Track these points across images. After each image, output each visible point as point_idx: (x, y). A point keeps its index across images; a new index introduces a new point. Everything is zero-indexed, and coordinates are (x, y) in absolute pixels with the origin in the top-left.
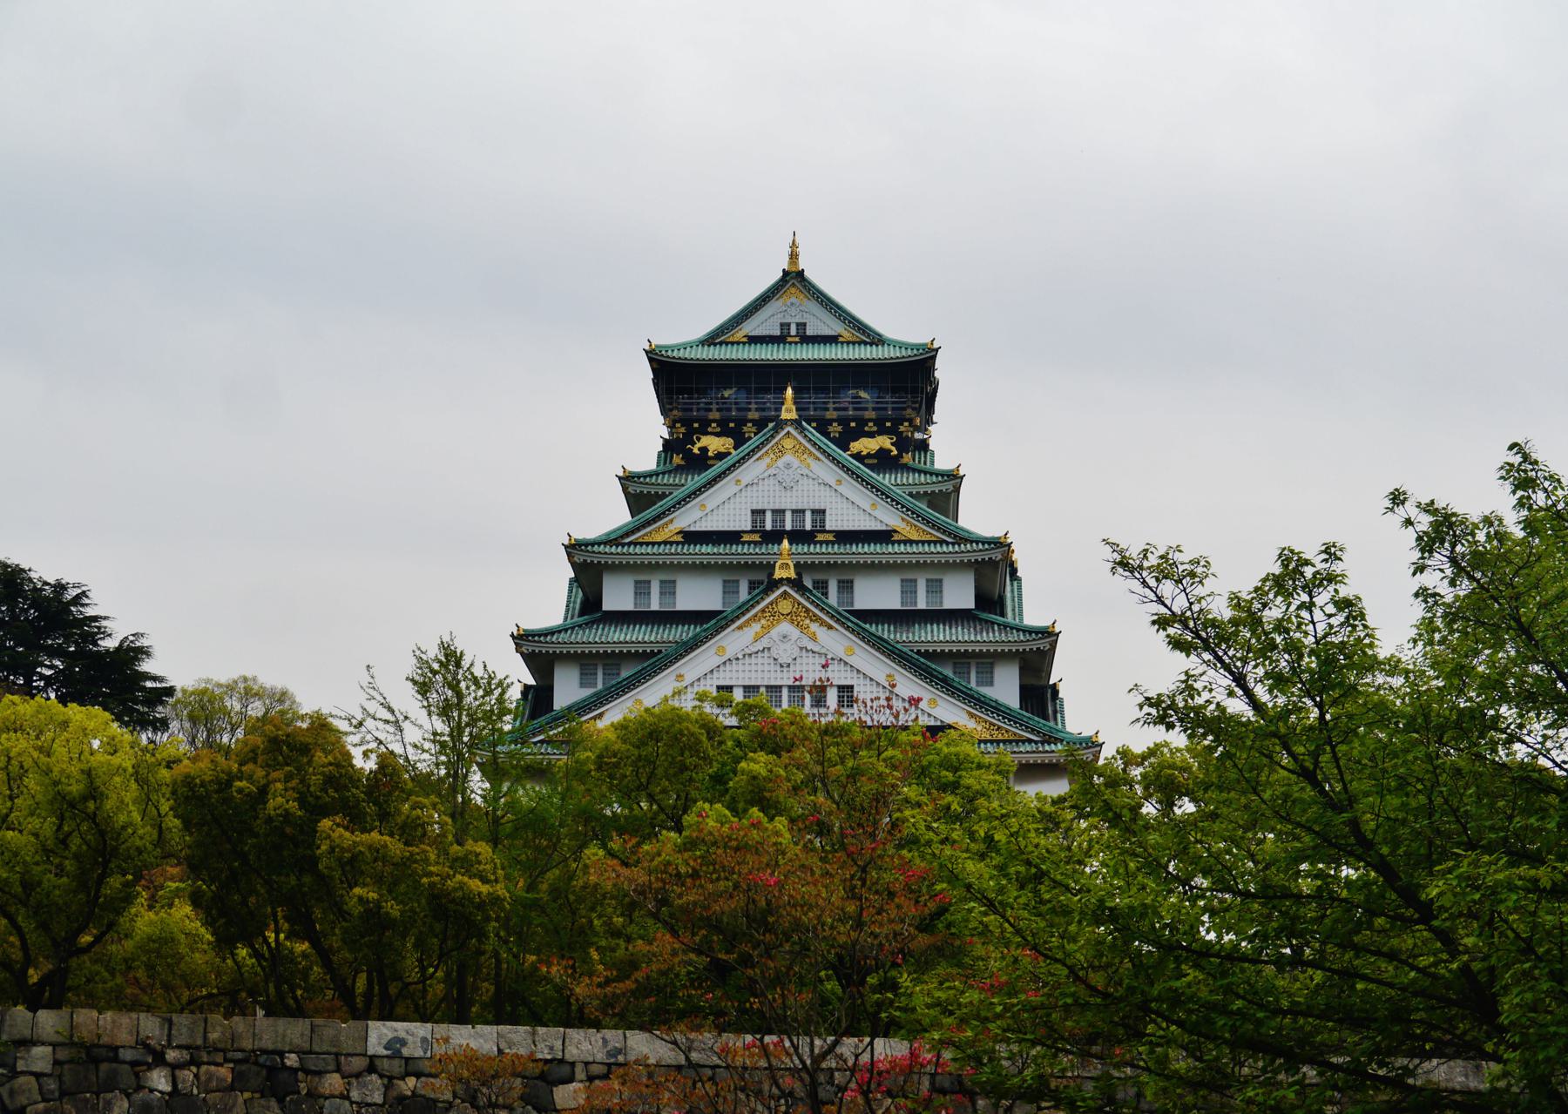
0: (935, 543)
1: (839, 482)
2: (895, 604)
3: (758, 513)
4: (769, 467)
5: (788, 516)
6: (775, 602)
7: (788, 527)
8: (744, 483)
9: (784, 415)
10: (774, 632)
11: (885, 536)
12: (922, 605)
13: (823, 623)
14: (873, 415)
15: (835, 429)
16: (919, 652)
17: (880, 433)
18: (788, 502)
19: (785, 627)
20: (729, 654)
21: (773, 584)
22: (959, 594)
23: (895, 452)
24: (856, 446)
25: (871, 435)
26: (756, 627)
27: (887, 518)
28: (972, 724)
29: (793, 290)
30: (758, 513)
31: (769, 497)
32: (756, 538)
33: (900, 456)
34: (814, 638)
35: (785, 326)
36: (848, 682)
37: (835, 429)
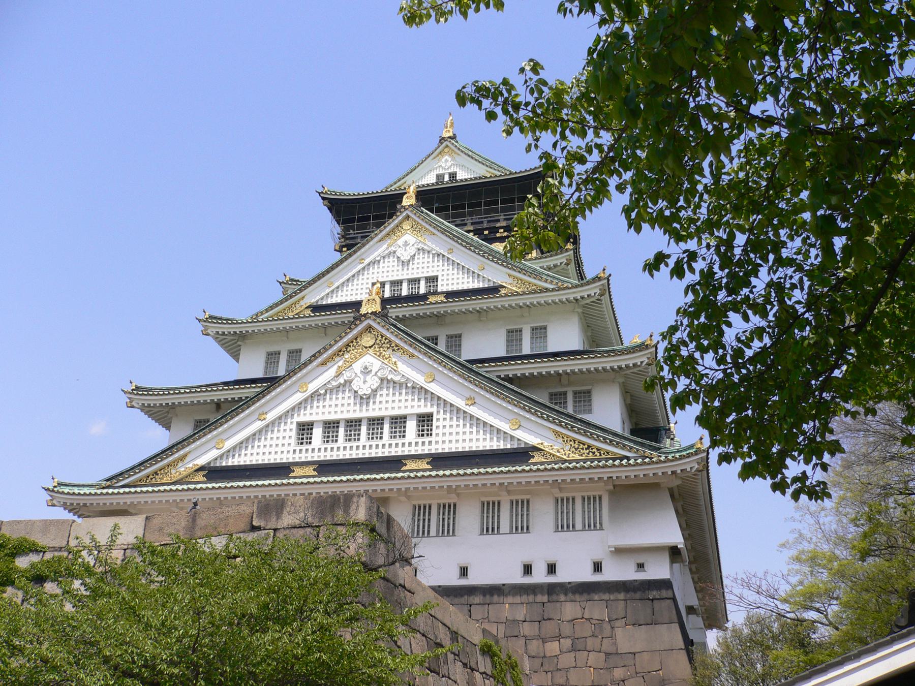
0: (541, 291)
2: (502, 353)
5: (405, 285)
7: (405, 293)
10: (357, 366)
11: (493, 290)
12: (526, 350)
13: (405, 352)
14: (504, 224)
19: (370, 360)
20: (312, 387)
21: (359, 318)
22: (566, 336)
27: (497, 275)
29: (446, 150)
31: (389, 271)
35: (440, 177)
36: (428, 410)
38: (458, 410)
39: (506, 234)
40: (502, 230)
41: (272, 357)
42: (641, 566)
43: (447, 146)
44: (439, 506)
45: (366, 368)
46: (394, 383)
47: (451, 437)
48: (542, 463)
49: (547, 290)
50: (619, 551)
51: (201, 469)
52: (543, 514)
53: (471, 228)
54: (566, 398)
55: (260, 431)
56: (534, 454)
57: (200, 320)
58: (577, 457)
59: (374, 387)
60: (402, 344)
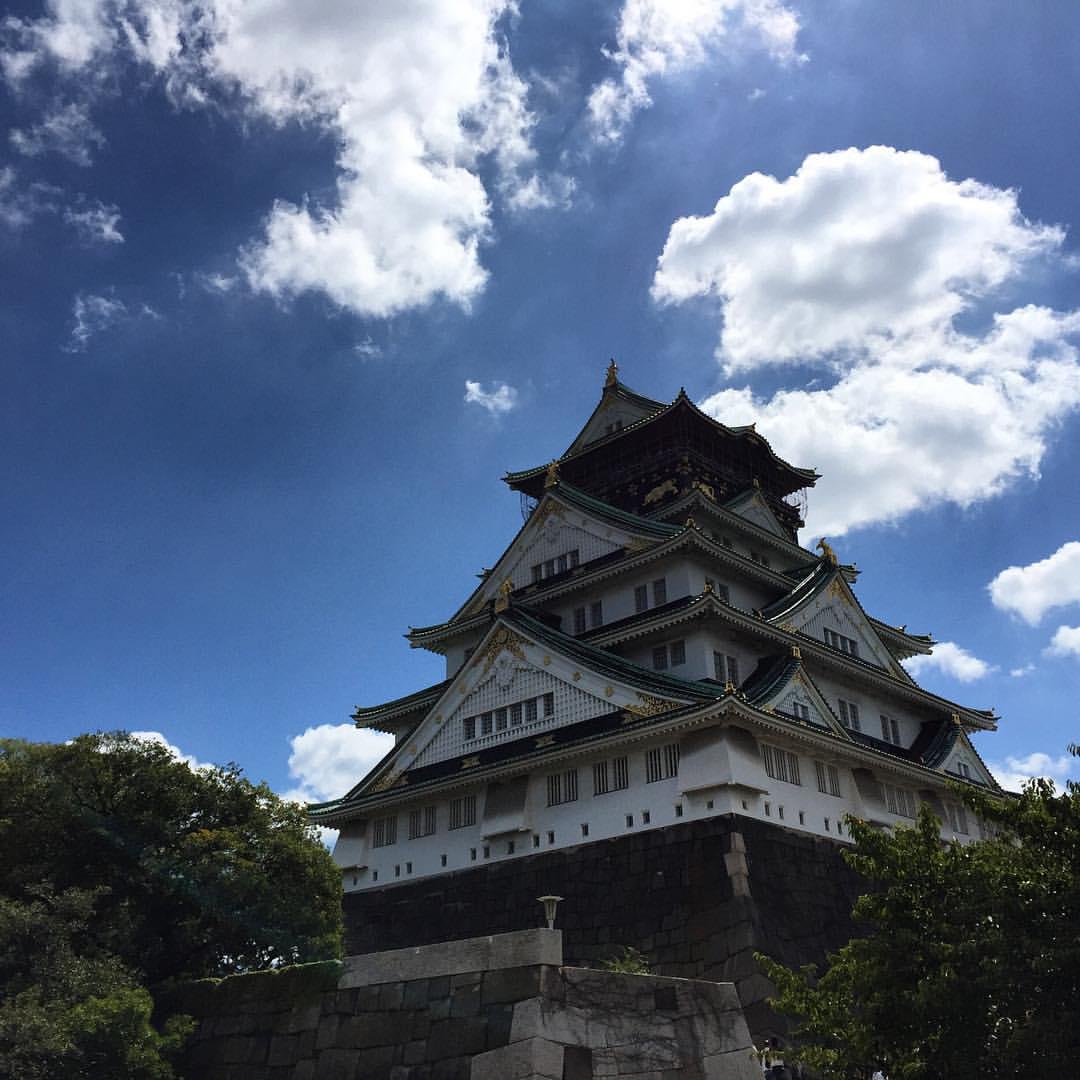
1: (584, 523)
2: (633, 612)
3: (536, 569)
4: (539, 530)
6: (495, 635)
7: (556, 572)
8: (524, 549)
9: (547, 485)
10: (497, 662)
11: (619, 555)
12: (651, 605)
15: (633, 490)
16: (608, 649)
17: (664, 480)
18: (554, 552)
19: (505, 654)
20: (468, 690)
21: (493, 617)
23: (676, 491)
24: (649, 498)
25: (658, 484)
26: (485, 660)
27: (621, 539)
28: (640, 703)
30: (536, 569)
32: (534, 588)
33: (680, 491)
34: (523, 658)
37: (633, 490)
38: (570, 686)
39: (659, 478)
40: (655, 475)
41: (469, 653)
42: (711, 805)
43: (611, 397)
44: (565, 774)
45: (502, 662)
46: (525, 671)
47: (570, 712)
48: (630, 724)
49: (658, 545)
50: (692, 794)
51: (405, 773)
52: (637, 767)
53: (630, 479)
54: (665, 652)
55: (440, 732)
56: (625, 716)
57: (407, 636)
58: (655, 713)
59: (510, 678)
60: (526, 637)
